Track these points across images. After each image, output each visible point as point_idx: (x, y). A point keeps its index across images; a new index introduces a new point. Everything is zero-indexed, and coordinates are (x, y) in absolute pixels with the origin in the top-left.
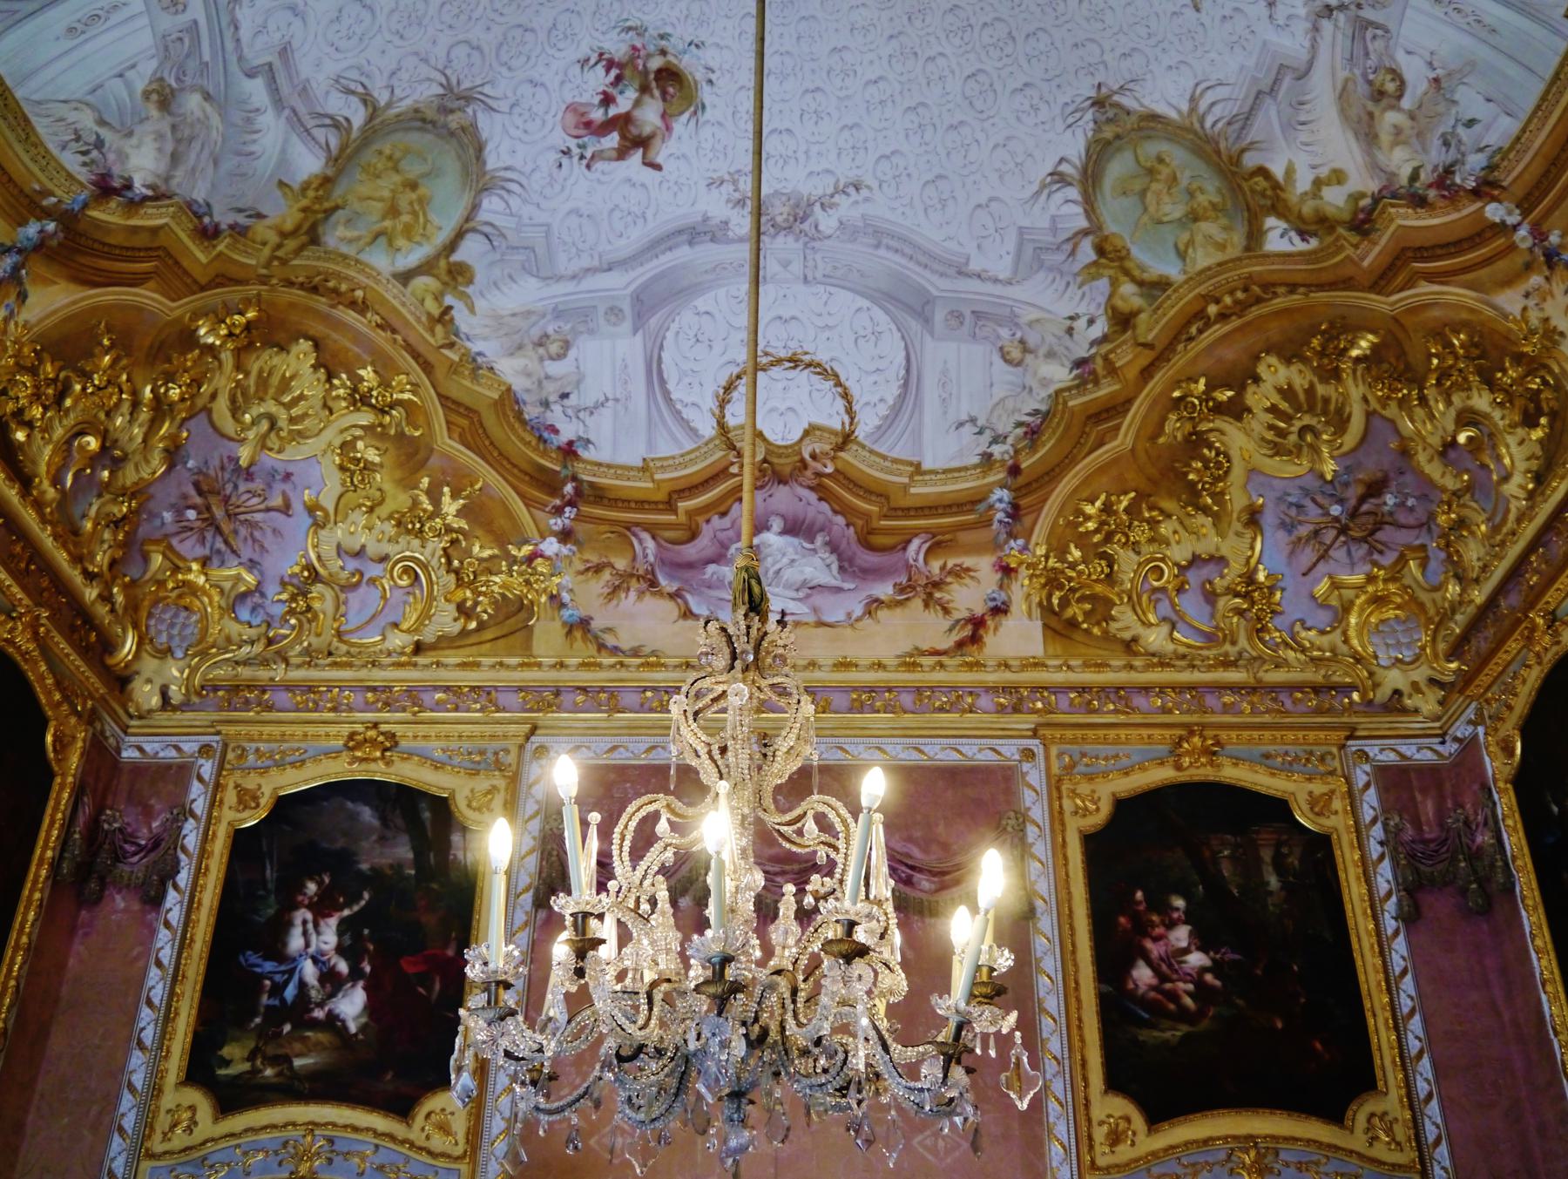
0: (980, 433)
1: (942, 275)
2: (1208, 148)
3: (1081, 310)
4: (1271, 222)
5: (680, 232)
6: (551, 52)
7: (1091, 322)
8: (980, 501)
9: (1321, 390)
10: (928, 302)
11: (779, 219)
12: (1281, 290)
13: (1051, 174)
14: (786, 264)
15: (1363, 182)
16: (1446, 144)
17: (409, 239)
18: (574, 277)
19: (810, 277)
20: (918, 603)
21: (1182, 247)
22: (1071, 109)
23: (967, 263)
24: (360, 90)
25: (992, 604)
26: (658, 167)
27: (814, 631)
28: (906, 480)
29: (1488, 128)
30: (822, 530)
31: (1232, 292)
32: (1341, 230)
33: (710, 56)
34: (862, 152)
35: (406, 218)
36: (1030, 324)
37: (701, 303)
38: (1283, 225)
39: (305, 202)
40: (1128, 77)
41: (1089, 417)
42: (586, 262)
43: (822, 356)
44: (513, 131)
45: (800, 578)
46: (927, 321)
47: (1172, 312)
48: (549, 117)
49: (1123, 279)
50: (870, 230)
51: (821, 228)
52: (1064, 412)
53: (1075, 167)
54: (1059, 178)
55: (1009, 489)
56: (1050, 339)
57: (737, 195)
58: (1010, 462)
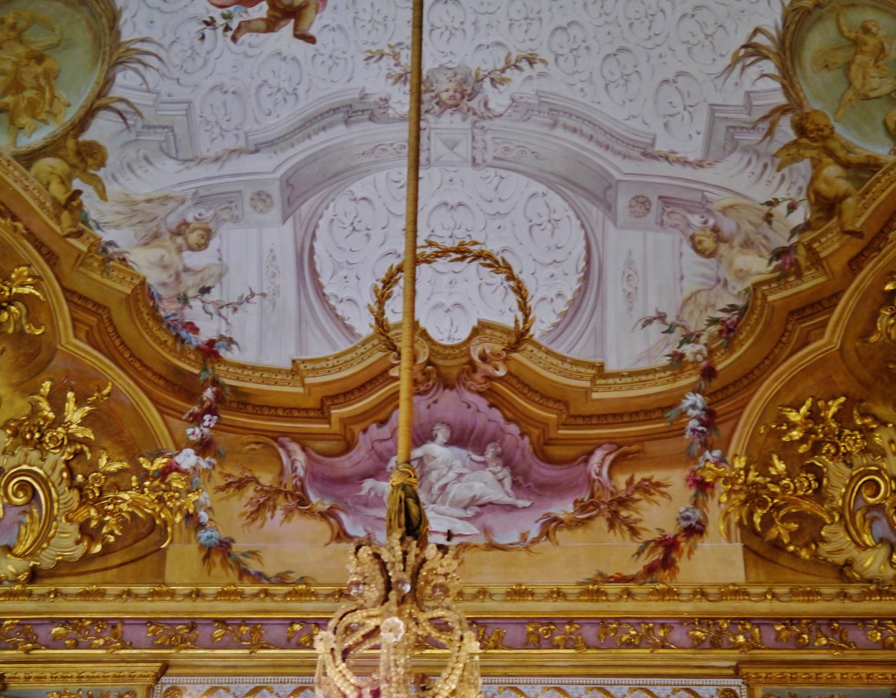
0: (669, 331)
3: (781, 194)
5: (335, 110)
7: (792, 208)
8: (670, 407)
10: (610, 187)
11: (445, 96)
13: (744, 47)
14: (452, 146)
17: (34, 116)
18: (217, 159)
19: (479, 160)
20: (601, 523)
23: (653, 144)
25: (685, 524)
26: (311, 40)
27: (484, 554)
28: (587, 384)
30: (493, 440)
34: (536, 23)
35: (29, 93)
36: (724, 210)
37: (358, 188)
41: (792, 313)
42: (231, 143)
43: (493, 247)
45: (467, 495)
46: (609, 208)
47: (883, 197)
49: (827, 160)
50: (545, 108)
51: (491, 105)
52: (763, 307)
53: (771, 38)
54: (752, 50)
55: (703, 394)
56: (747, 228)
57: (399, 70)
58: (704, 364)
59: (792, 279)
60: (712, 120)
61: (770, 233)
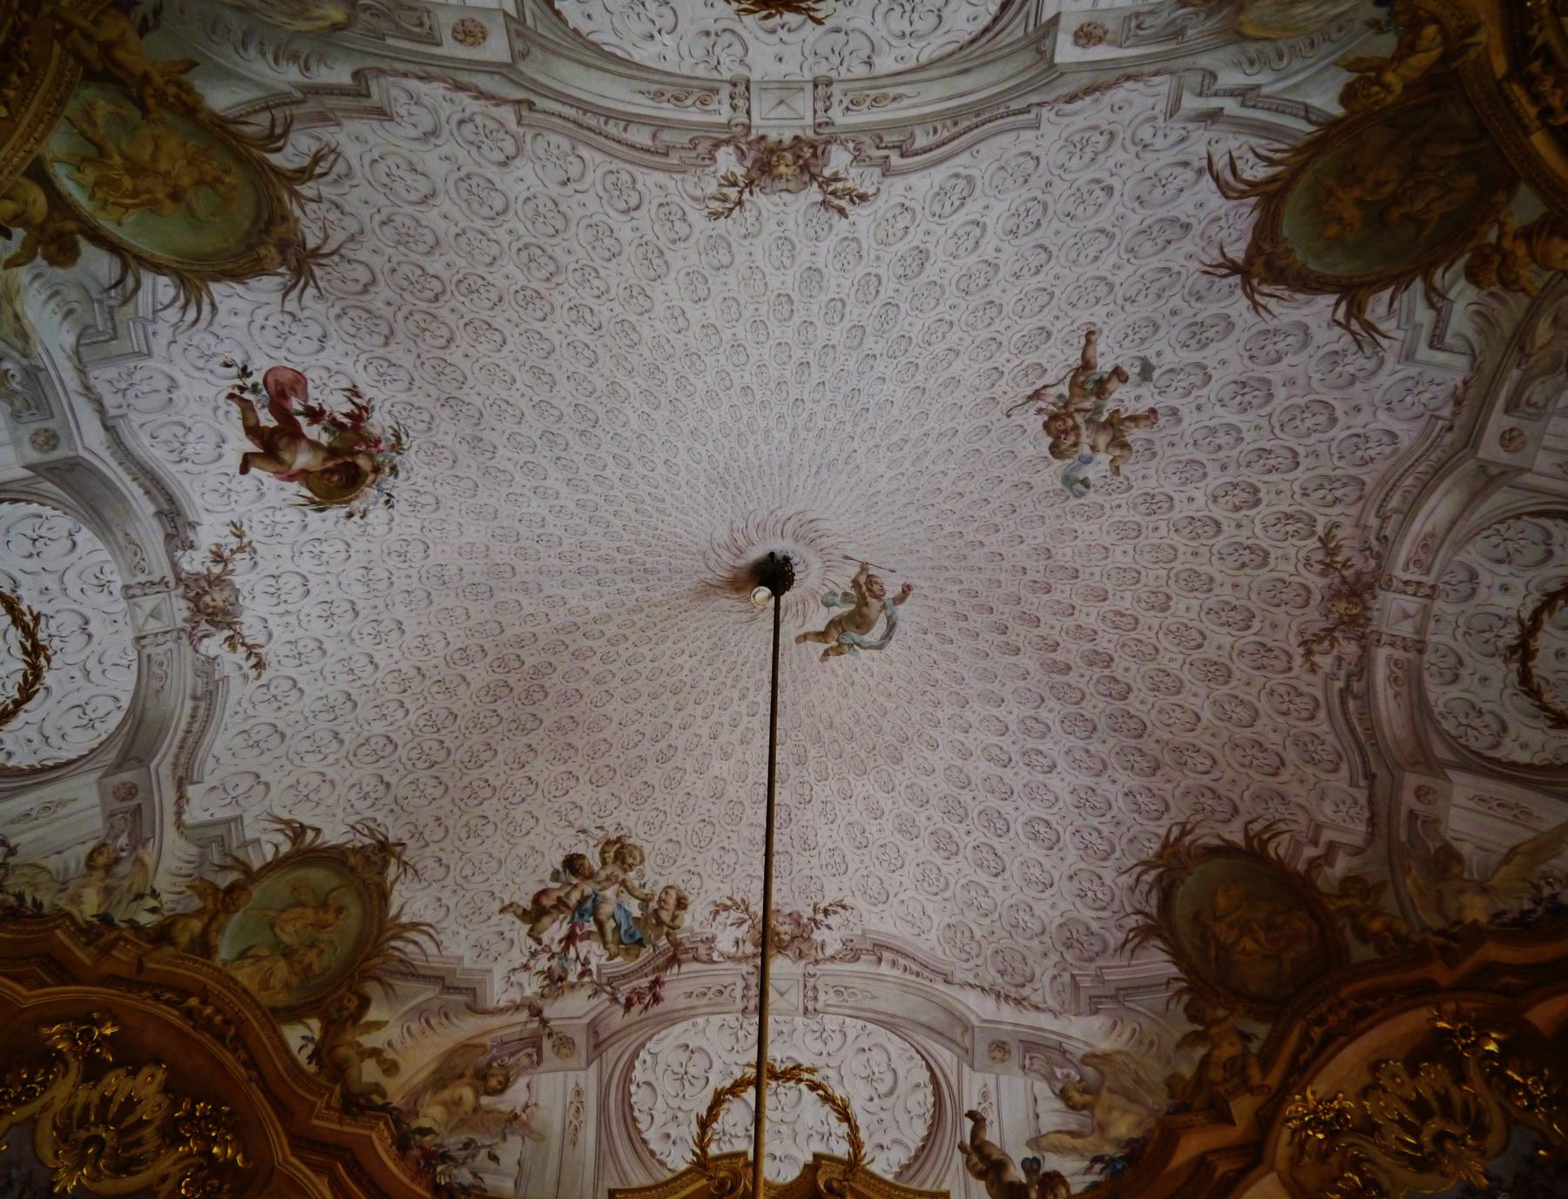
1: (175, 765)
2: (369, 948)
3: (165, 897)
4: (315, 1024)
5: (170, 499)
6: (363, 358)
7: (153, 910)
9: (148, 1132)
10: (140, 761)
11: (207, 599)
12: (242, 1054)
13: (301, 825)
14: (155, 615)
15: (396, 1090)
16: (466, 1146)
17: (97, 184)
18: (87, 388)
19: (144, 642)
21: (251, 953)
22: (373, 825)
23: (192, 783)
24: (318, 170)
26: (244, 470)
29: (497, 1172)
31: (218, 1011)
32: (338, 1088)
33: (378, 514)
34: (297, 662)
35: (127, 183)
36: (139, 861)
37: (85, 536)
38: (317, 1036)
39: (158, 80)
40: (419, 867)
42: (110, 401)
43: (49, 678)
44: (260, 315)
46: (119, 767)
47: (180, 971)
48: (283, 353)
49: (206, 918)
50: (211, 687)
51: (206, 641)
53: (313, 841)
54: (298, 831)
56: (126, 884)
57: (227, 553)
59: (83, 939)
60: (226, 822)
61: (124, 903)
